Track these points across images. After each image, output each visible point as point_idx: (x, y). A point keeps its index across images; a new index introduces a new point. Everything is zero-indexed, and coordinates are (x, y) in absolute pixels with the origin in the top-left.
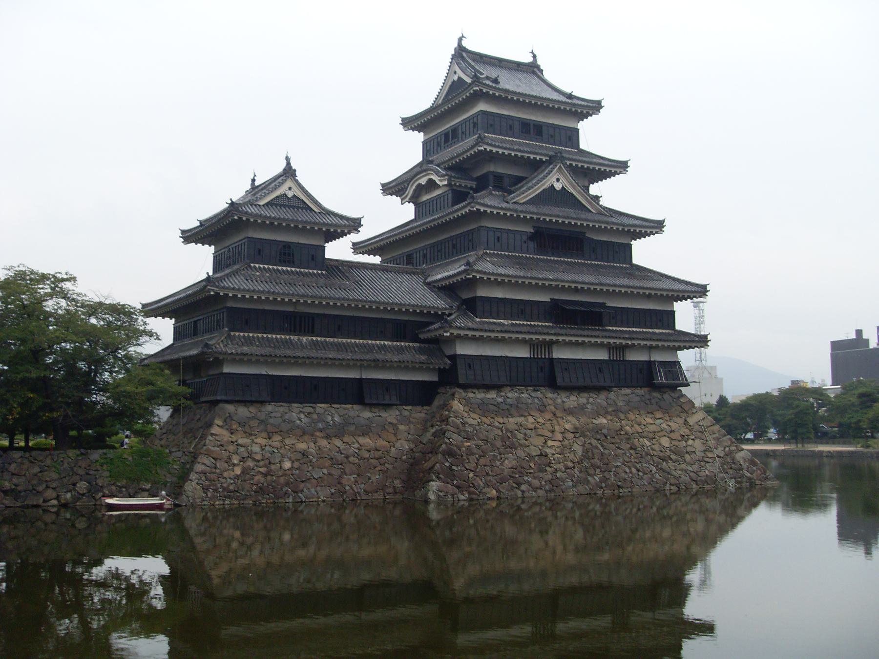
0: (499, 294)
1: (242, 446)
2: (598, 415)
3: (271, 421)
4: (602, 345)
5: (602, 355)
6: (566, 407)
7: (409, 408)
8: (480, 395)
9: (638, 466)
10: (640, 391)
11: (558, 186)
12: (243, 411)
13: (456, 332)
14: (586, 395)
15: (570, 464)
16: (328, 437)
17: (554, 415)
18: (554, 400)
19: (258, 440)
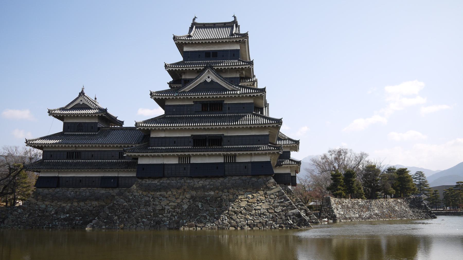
0: (162, 135)
1: (38, 205)
2: (211, 189)
3: (57, 195)
4: (220, 155)
5: (220, 160)
6: (195, 186)
7: (125, 189)
8: (148, 182)
9: (216, 216)
10: (244, 178)
11: (209, 80)
12: (46, 191)
13: (129, 154)
14: (209, 180)
15: (174, 214)
16: (78, 202)
17: (185, 190)
18: (189, 183)
19: (46, 203)
